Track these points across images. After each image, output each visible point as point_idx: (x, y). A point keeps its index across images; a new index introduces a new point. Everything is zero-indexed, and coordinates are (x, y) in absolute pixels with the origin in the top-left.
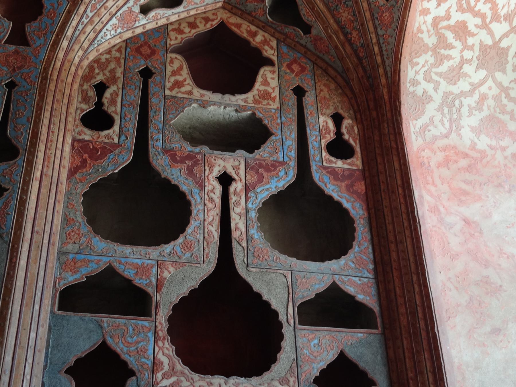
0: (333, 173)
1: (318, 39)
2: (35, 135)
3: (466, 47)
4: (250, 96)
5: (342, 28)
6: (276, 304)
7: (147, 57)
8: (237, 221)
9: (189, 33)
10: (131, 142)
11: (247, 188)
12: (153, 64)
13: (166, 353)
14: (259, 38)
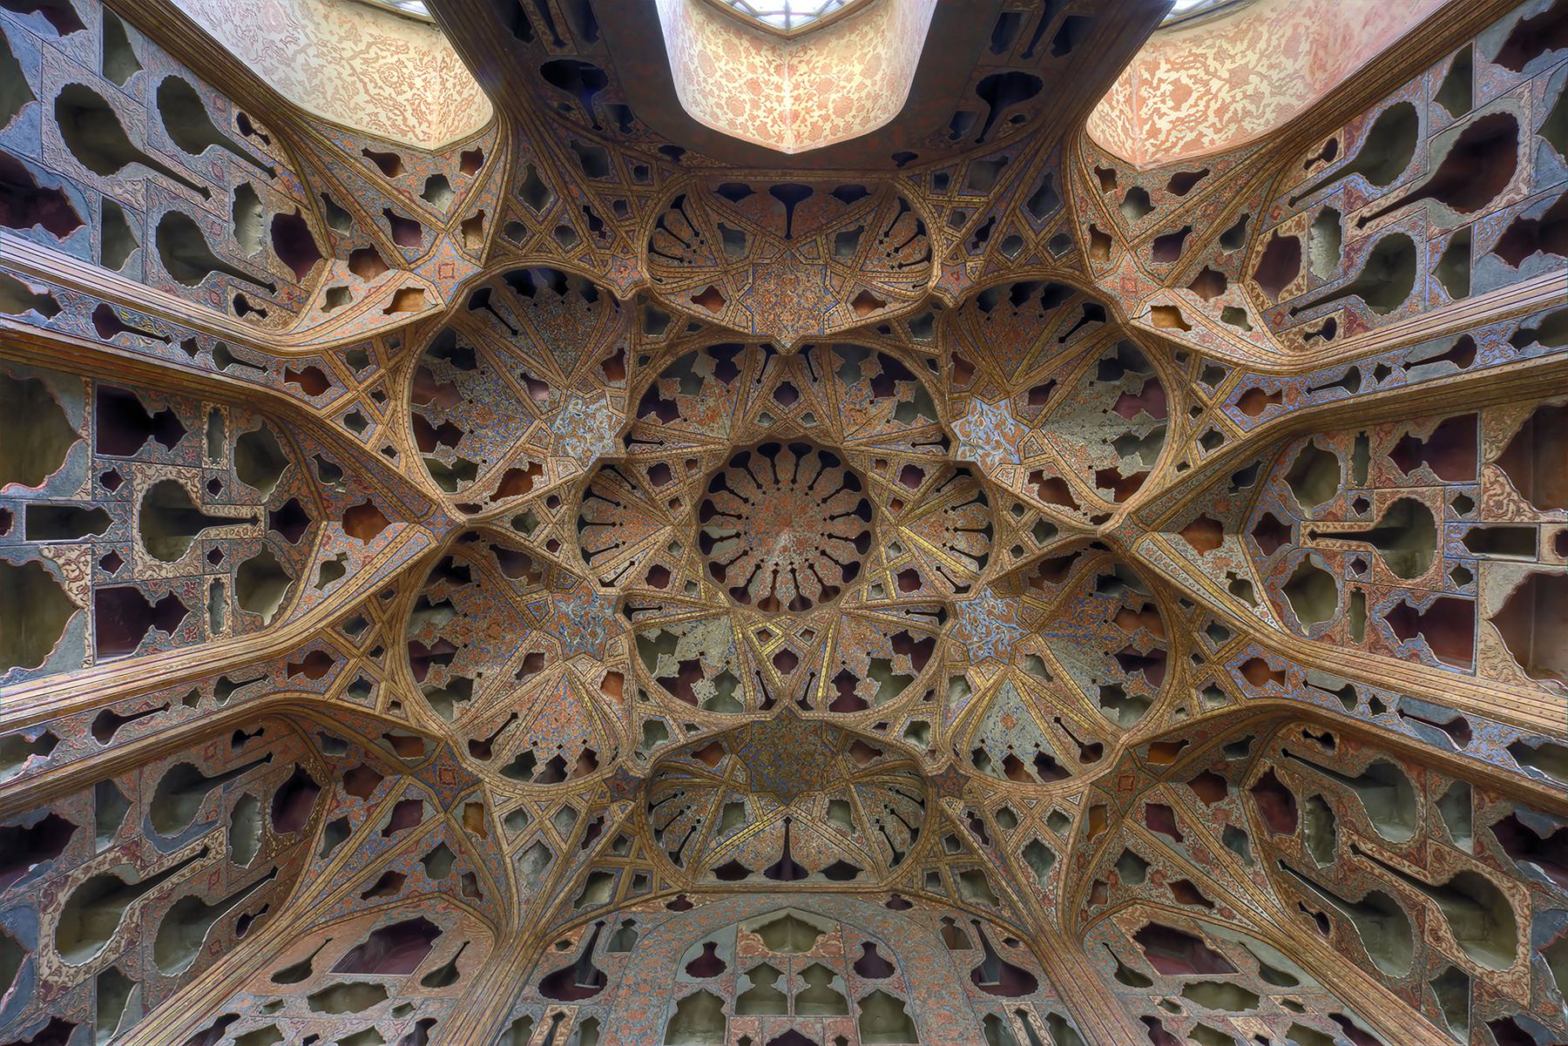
0: (1348, 148)
1: (1251, 207)
2: (1339, 361)
3: (1234, 100)
4: (1300, 235)
5: (1238, 193)
6: (1455, 136)
7: (1283, 316)
8: (1392, 199)
9: (1264, 296)
10: (1342, 301)
11: (1366, 203)
12: (1287, 309)
13: (1499, 202)
14: (1260, 248)
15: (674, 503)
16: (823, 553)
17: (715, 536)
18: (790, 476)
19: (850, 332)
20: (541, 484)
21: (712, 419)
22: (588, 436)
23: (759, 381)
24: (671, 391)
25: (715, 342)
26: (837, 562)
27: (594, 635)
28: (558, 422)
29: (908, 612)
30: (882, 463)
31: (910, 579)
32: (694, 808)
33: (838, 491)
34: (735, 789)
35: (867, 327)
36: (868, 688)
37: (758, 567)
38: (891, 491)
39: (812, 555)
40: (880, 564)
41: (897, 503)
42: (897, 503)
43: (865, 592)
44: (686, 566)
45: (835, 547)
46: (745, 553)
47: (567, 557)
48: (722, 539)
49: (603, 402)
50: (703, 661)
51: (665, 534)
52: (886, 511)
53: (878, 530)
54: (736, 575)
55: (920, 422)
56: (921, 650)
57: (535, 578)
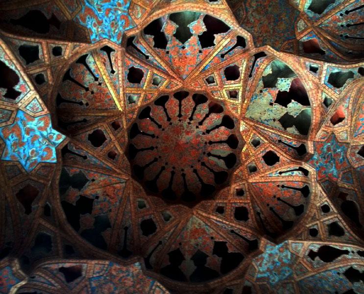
15: (240, 193)
16: (169, 119)
17: (222, 161)
18: (164, 173)
19: (92, 257)
20: (315, 246)
21: (196, 231)
22: (276, 260)
23: (160, 243)
24: (214, 261)
25: (180, 284)
26: (165, 110)
27: (329, 149)
28: (287, 274)
29: (147, 57)
30: (112, 156)
31: (134, 76)
32: (340, 24)
33: (142, 150)
34: (309, 19)
35: (81, 257)
36: (198, 27)
37: (208, 132)
38: (115, 136)
39: (176, 122)
40: (146, 96)
41: (115, 126)
42: (115, 126)
43: (162, 87)
44: (251, 155)
45: (161, 119)
46: (211, 143)
47: (319, 196)
48: (219, 157)
49: (260, 276)
50: (274, 100)
51: (254, 179)
52: (125, 125)
53: (135, 116)
54: (223, 133)
55: (73, 171)
56: (154, 29)
57: (343, 196)
